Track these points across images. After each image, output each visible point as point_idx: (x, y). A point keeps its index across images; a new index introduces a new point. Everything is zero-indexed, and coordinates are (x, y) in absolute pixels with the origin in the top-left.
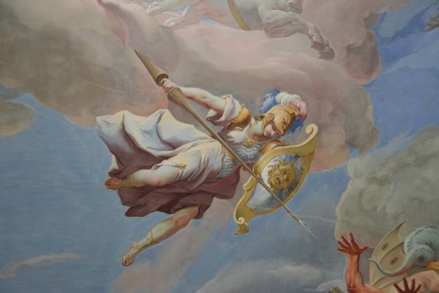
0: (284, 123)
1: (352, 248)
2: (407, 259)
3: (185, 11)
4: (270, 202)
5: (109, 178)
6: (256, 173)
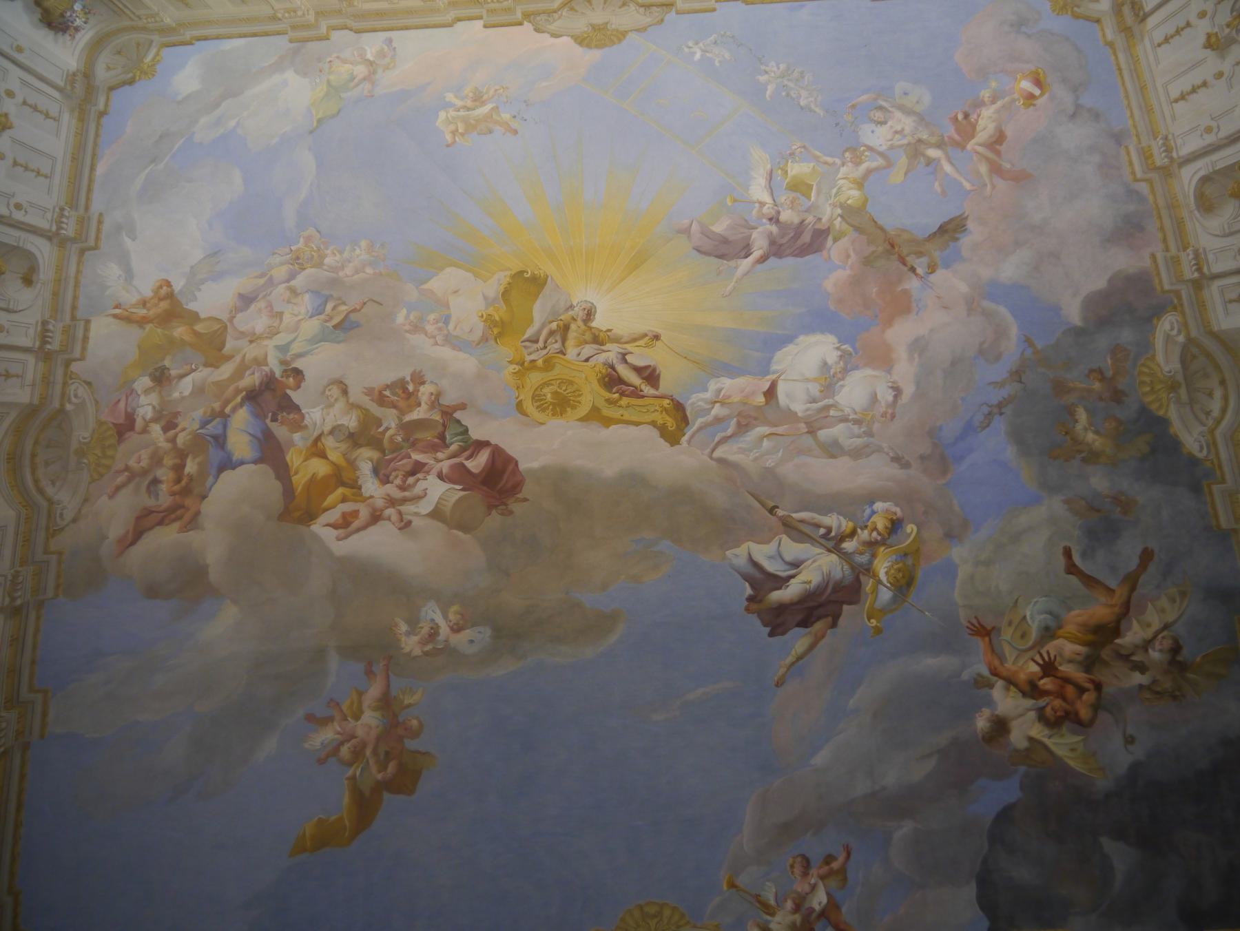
0: (886, 528)
1: (983, 631)
2: (1034, 635)
3: (780, 454)
4: (894, 600)
5: (746, 603)
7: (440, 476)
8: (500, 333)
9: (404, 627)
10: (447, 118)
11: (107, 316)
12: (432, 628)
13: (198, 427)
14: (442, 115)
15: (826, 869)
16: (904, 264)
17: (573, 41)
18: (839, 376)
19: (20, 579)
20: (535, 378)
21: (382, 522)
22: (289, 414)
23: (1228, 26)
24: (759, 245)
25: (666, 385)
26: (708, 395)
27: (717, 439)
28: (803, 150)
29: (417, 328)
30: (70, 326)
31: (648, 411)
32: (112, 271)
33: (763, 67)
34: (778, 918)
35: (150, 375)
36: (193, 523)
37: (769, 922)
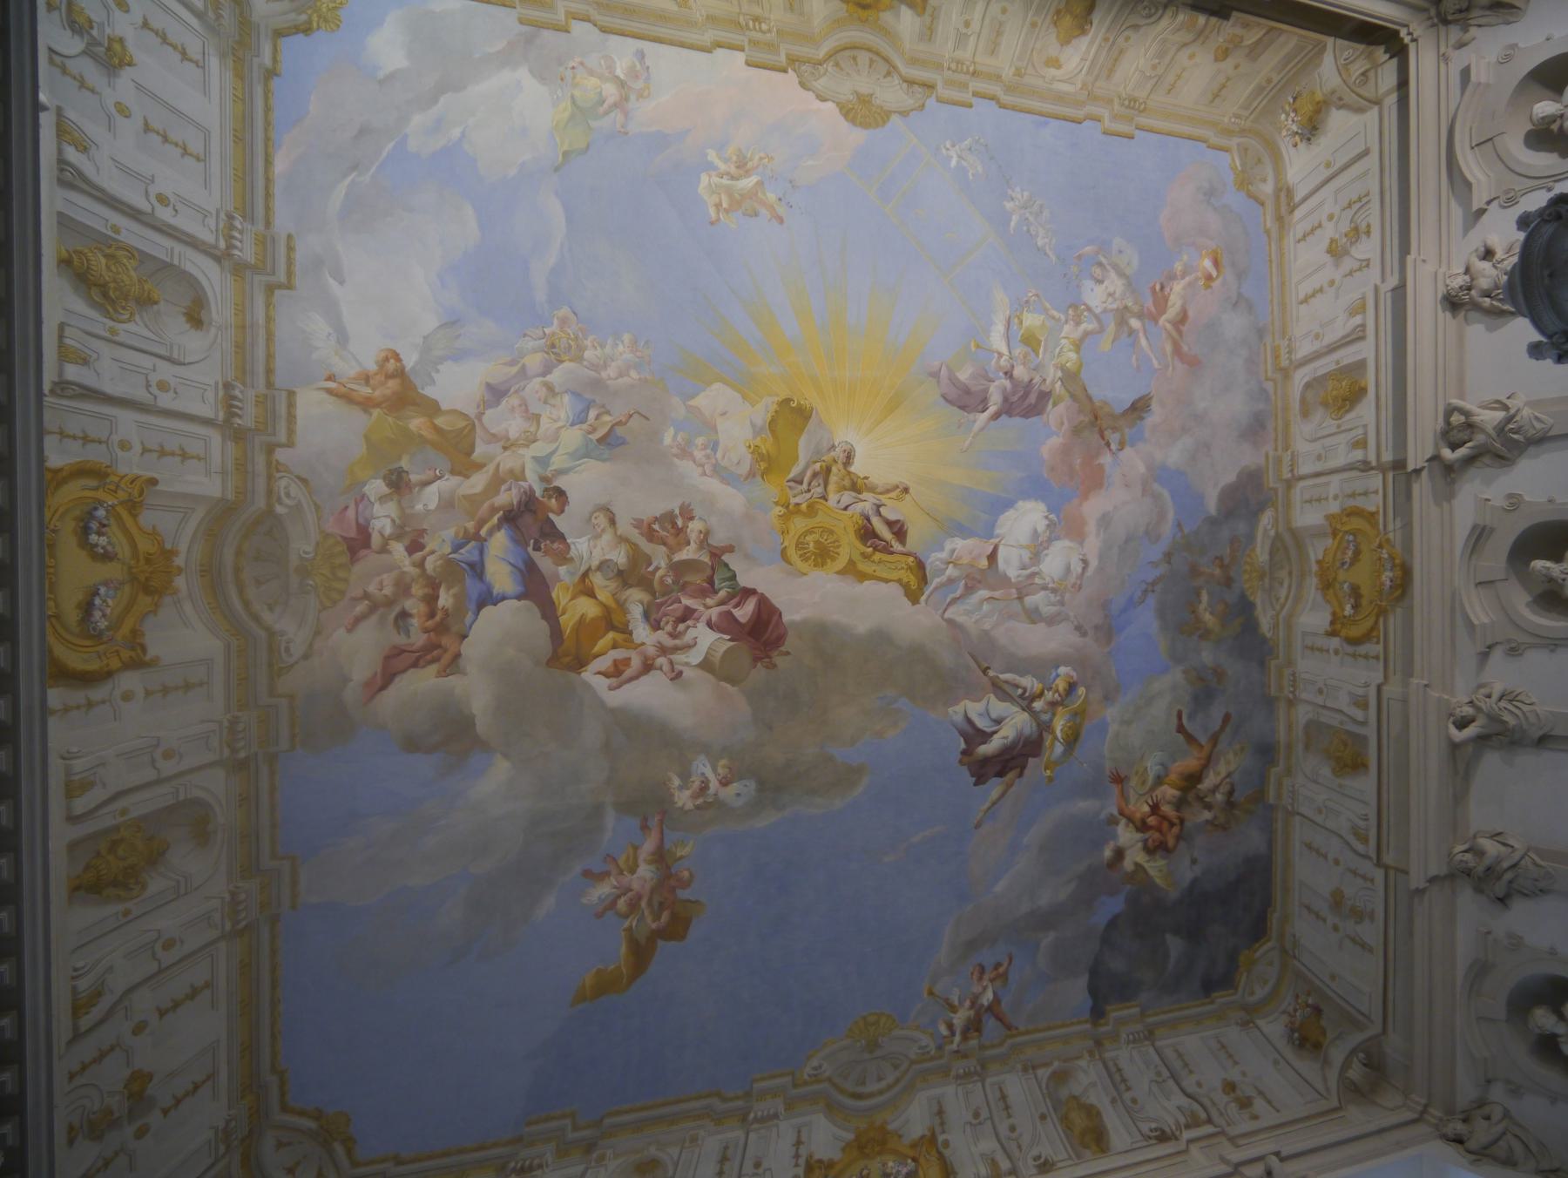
0: (1065, 690)
6: (1053, 732)
7: (709, 624)
9: (676, 782)
10: (710, 184)
12: (703, 782)
13: (449, 550)
14: (704, 178)
15: (995, 973)
16: (1103, 438)
17: (838, 110)
18: (1045, 545)
19: (240, 727)
20: (799, 524)
21: (652, 672)
22: (553, 542)
23: (1346, 235)
25: (914, 540)
26: (944, 555)
27: (948, 600)
28: (1036, 299)
29: (685, 453)
30: (266, 396)
31: (896, 568)
32: (318, 326)
33: (1010, 192)
35: (384, 478)
36: (453, 665)
37: (952, 1018)
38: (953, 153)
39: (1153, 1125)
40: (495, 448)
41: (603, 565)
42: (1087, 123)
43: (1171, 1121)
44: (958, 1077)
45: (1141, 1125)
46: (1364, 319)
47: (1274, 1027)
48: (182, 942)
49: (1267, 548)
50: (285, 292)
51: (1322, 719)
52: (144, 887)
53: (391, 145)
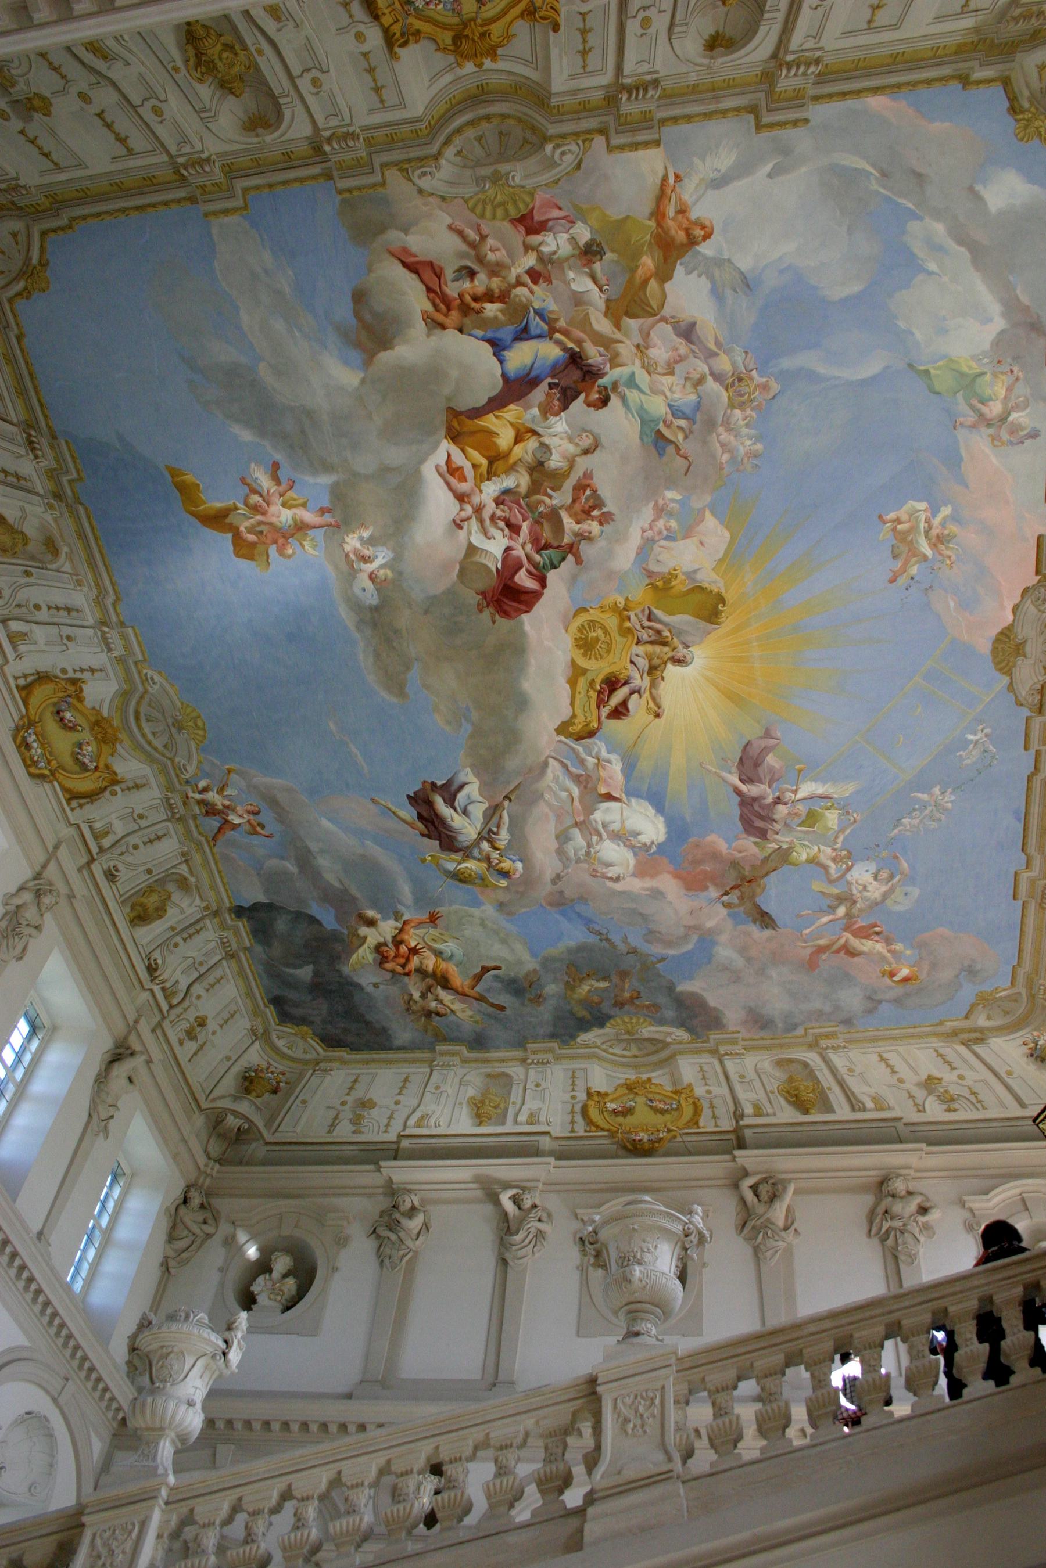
1: (433, 919)
2: (435, 946)
6: (464, 861)
7: (508, 549)
8: (657, 586)
9: (366, 534)
11: (666, 168)
13: (536, 307)
14: (922, 506)
16: (732, 888)
19: (351, 143)
20: (612, 622)
21: (457, 503)
22: (559, 400)
23: (946, 1091)
24: (751, 790)
26: (604, 754)
27: (564, 761)
29: (660, 511)
32: (724, 160)
33: (950, 790)
34: (217, 796)
35: (592, 240)
36: (435, 325)
38: (979, 735)
39: (159, 962)
40: (637, 339)
41: (545, 447)
42: (1024, 856)
43: (165, 976)
44: (168, 799)
45: (158, 951)
46: (870, 1110)
47: (255, 1056)
48: (161, 122)
49: (657, 1036)
50: (753, 123)
51: (514, 1088)
52: (201, 81)
53: (910, 205)
